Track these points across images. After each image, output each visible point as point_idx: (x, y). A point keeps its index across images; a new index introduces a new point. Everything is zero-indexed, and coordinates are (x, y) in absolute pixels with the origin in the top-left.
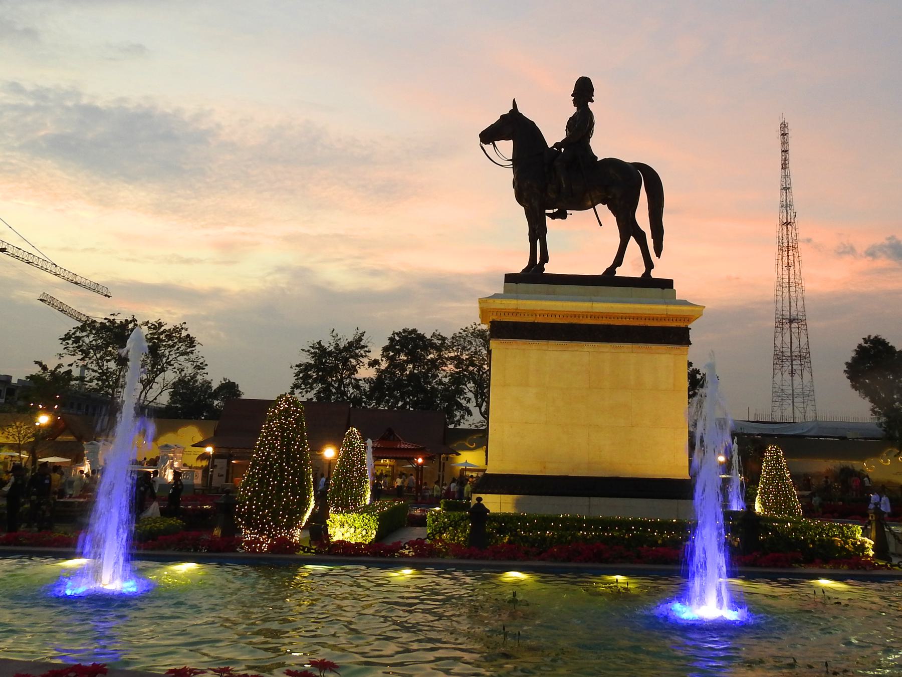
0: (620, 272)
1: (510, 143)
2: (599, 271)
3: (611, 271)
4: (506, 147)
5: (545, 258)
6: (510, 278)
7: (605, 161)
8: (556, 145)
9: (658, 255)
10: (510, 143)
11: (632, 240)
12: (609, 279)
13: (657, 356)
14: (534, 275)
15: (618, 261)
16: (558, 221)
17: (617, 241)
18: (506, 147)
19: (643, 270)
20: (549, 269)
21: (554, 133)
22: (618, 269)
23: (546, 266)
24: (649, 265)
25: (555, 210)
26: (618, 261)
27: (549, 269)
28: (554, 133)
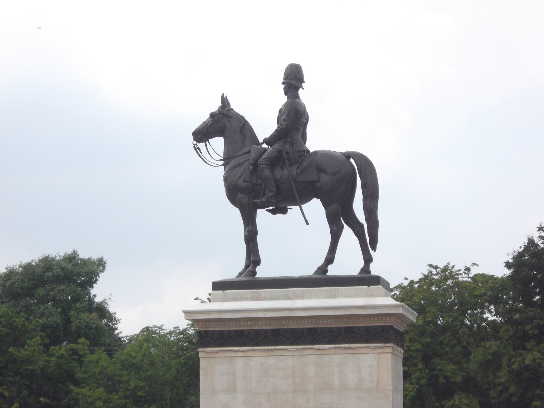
0: (333, 271)
1: (222, 139)
3: (323, 269)
4: (218, 144)
5: (257, 262)
6: (218, 286)
7: (316, 153)
8: (266, 141)
9: (374, 249)
10: (222, 139)
11: (348, 235)
12: (321, 279)
13: (361, 356)
14: (249, 280)
15: (330, 260)
16: (279, 216)
17: (329, 238)
18: (218, 144)
19: (361, 263)
20: (263, 272)
22: (330, 267)
23: (258, 269)
24: (368, 259)
25: (273, 207)
26: (330, 260)
27: (263, 272)
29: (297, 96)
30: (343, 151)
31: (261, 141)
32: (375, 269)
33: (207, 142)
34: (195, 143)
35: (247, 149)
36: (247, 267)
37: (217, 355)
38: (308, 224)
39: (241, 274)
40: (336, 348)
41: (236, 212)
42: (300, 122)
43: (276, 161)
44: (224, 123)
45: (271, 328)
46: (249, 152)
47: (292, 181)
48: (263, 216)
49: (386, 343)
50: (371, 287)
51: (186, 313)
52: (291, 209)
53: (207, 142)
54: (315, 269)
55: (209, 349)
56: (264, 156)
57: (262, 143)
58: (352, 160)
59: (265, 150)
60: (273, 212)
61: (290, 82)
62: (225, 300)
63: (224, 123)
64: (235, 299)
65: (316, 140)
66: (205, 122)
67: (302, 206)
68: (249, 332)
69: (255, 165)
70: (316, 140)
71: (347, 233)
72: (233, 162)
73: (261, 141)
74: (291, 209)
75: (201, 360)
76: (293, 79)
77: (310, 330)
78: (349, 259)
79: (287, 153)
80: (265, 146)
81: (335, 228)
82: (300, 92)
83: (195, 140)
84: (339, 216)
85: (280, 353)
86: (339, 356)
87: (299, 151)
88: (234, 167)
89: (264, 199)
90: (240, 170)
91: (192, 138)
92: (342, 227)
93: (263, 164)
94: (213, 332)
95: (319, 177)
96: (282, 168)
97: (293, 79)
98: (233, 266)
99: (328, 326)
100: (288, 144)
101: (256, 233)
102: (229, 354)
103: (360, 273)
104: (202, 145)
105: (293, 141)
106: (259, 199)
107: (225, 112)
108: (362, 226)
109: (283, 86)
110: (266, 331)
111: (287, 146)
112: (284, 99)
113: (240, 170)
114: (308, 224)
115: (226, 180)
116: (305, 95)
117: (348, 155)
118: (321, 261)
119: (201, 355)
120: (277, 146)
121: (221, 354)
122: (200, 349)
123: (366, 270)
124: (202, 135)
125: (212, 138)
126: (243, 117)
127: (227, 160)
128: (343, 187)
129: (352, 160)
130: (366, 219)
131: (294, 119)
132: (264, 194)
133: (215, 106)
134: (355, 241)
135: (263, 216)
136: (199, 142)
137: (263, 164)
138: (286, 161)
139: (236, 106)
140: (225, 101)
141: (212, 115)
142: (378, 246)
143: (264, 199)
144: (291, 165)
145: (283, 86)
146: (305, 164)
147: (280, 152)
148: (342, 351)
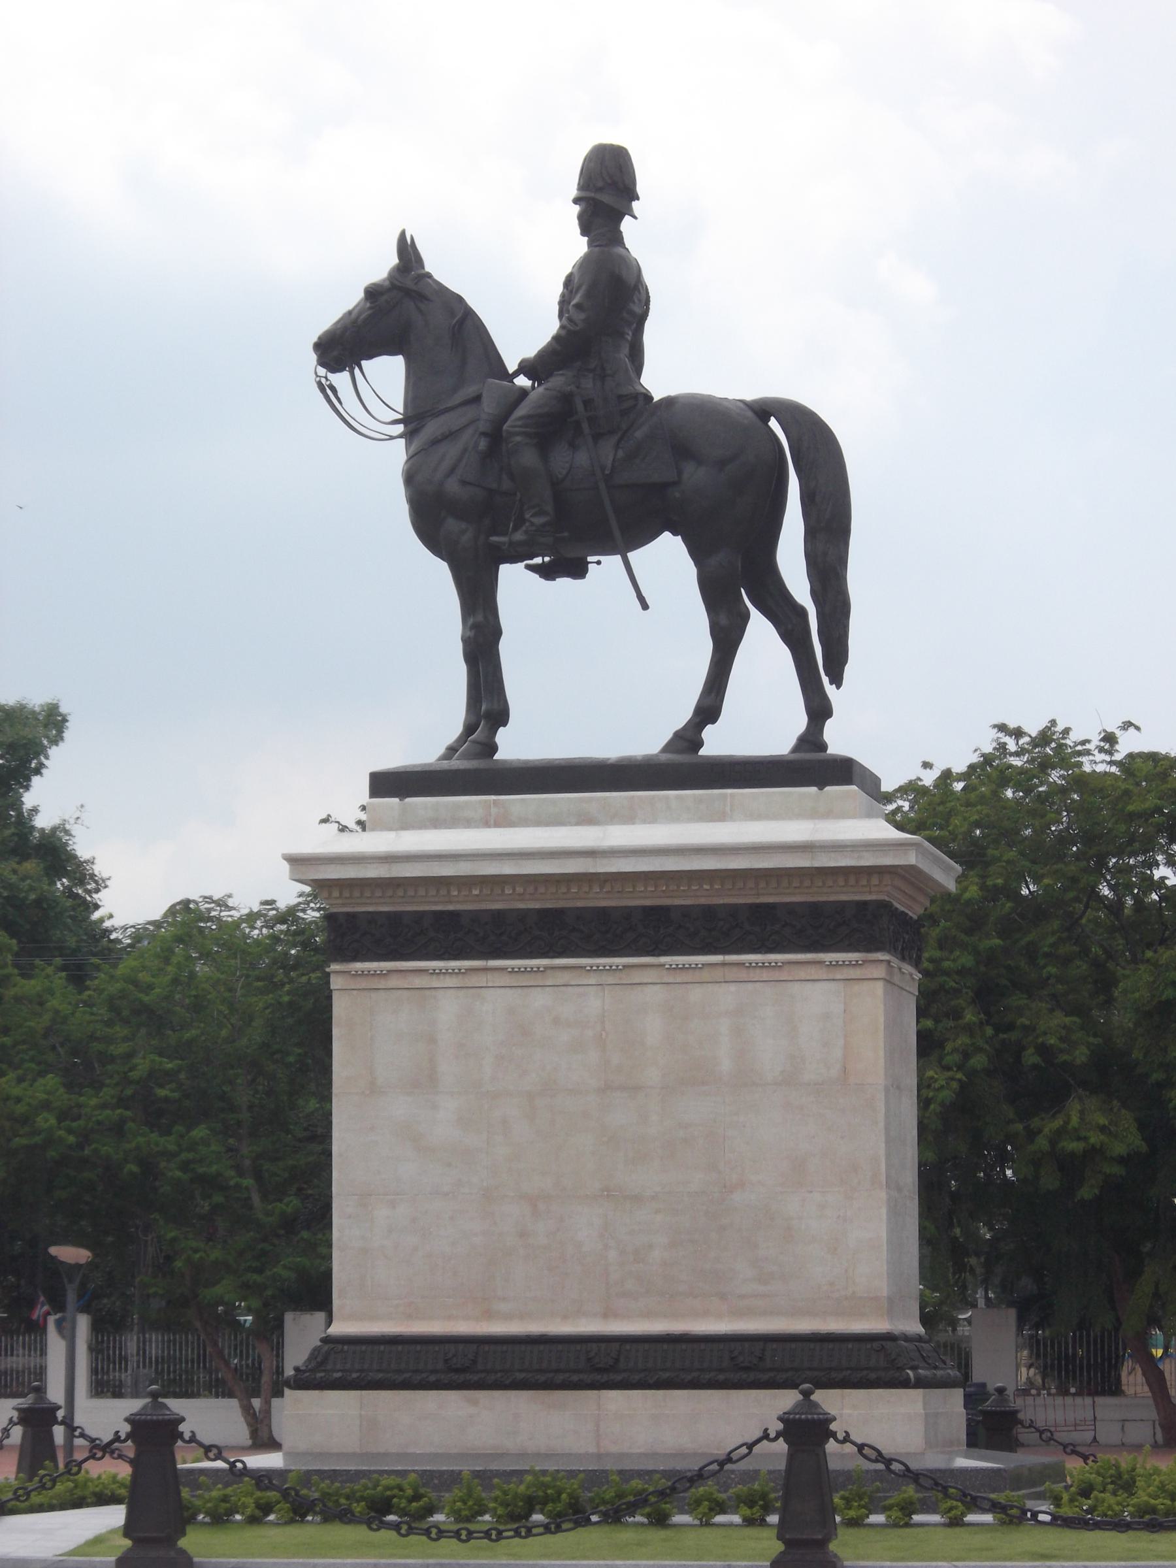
0: (718, 742)
2: (648, 740)
4: (387, 374)
5: (500, 716)
6: (387, 784)
7: (669, 402)
8: (526, 368)
9: (837, 680)
12: (683, 767)
13: (796, 988)
14: (476, 770)
15: (708, 710)
16: (564, 582)
18: (387, 374)
19: (799, 722)
20: (514, 745)
21: (522, 321)
22: (708, 733)
23: (503, 736)
24: (819, 710)
25: (547, 559)
26: (708, 710)
27: (514, 745)
28: (522, 321)
29: (618, 239)
30: (750, 396)
31: (512, 367)
32: (838, 739)
33: (357, 371)
34: (322, 371)
35: (469, 391)
36: (469, 729)
37: (382, 984)
38: (645, 606)
39: (452, 750)
40: (724, 964)
41: (441, 571)
42: (625, 315)
43: (556, 425)
44: (406, 316)
45: (537, 906)
46: (477, 399)
47: (602, 486)
48: (515, 582)
49: (869, 951)
50: (828, 788)
51: (295, 861)
52: (599, 563)
53: (357, 371)
54: (668, 736)
55: (359, 966)
56: (522, 411)
57: (516, 374)
58: (774, 424)
59: (524, 393)
60: (547, 572)
61: (598, 196)
62: (405, 824)
63: (406, 316)
64: (436, 823)
65: (673, 364)
66: (350, 313)
67: (630, 555)
68: (476, 916)
69: (495, 436)
70: (673, 364)
71: (760, 631)
72: (432, 428)
73: (512, 367)
74: (599, 563)
75: (335, 996)
76: (607, 188)
77: (649, 911)
78: (763, 709)
79: (587, 403)
80: (522, 381)
81: (724, 620)
82: (626, 225)
83: (322, 362)
84: (736, 582)
85: (565, 977)
86: (733, 988)
87: (620, 398)
88: (435, 442)
89: (519, 536)
90: (451, 451)
91: (314, 357)
92: (746, 617)
93: (518, 434)
94: (372, 917)
95: (680, 473)
96: (573, 446)
97: (607, 188)
98: (429, 727)
99: (703, 901)
100: (591, 375)
101: (497, 633)
102: (418, 981)
103: (795, 750)
104: (341, 380)
105: (603, 369)
106: (504, 534)
107: (409, 283)
108: (802, 612)
109: (577, 209)
110: (523, 915)
111: (588, 383)
112: (579, 246)
113: (451, 451)
114: (645, 606)
115: (410, 478)
116: (637, 234)
117: (763, 410)
118: (683, 715)
119: (336, 983)
120: (558, 381)
121: (394, 982)
122: (334, 967)
123: (812, 739)
124: (342, 349)
125: (370, 357)
126: (460, 299)
127: (414, 421)
128: (747, 500)
129: (774, 424)
130: (814, 594)
131: (607, 304)
132: (520, 521)
133: (381, 264)
134: (784, 655)
135: (515, 582)
136: (334, 370)
137: (518, 434)
138: (585, 426)
139: (441, 267)
140: (408, 252)
141: (372, 293)
142: (849, 671)
143: (519, 536)
144: (597, 437)
145: (577, 209)
146: (639, 434)
147: (566, 399)
148: (743, 974)
